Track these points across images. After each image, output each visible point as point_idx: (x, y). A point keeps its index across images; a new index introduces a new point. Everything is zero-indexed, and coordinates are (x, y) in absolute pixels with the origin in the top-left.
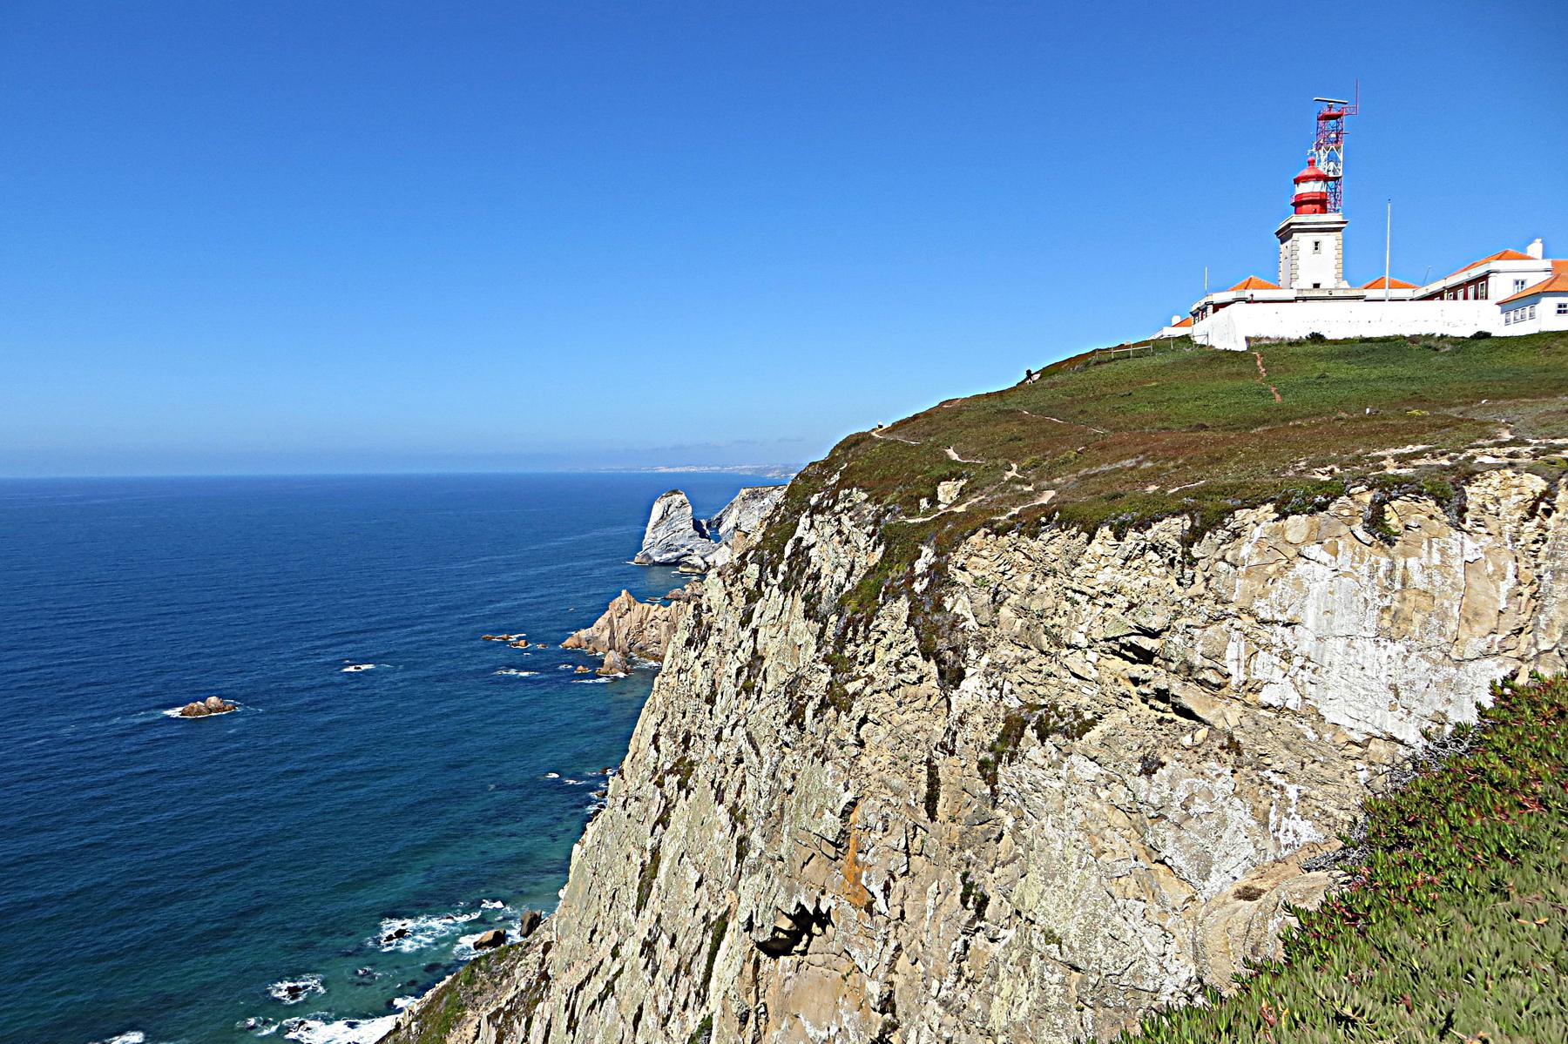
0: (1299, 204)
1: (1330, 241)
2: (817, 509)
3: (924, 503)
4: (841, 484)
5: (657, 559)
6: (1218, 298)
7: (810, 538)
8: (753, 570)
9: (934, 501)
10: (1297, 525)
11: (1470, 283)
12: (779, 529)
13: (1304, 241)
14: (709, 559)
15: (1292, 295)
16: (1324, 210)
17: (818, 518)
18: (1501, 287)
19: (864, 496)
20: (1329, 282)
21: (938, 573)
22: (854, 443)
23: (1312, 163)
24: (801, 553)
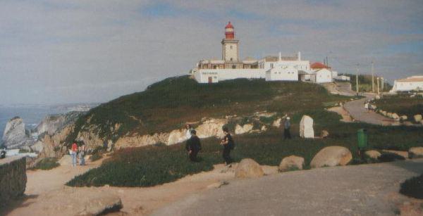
0: (227, 34)
1: (234, 46)
2: (84, 130)
4: (92, 122)
9: (114, 128)
14: (33, 147)
15: (222, 62)
20: (235, 59)
21: (113, 146)
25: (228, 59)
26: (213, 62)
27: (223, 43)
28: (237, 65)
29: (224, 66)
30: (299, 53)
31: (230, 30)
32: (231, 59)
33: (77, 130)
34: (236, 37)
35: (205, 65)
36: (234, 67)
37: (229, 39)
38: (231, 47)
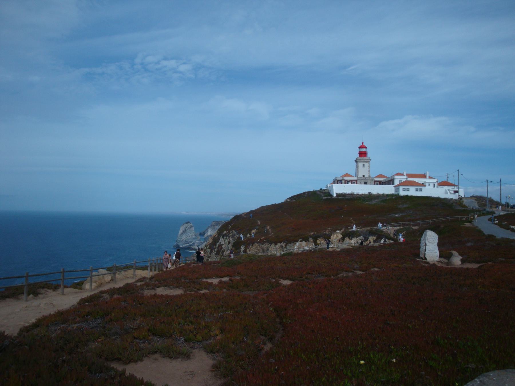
1: (366, 164)
2: (225, 235)
3: (249, 235)
5: (181, 246)
6: (338, 179)
7: (223, 242)
8: (209, 250)
9: (250, 234)
10: (304, 243)
11: (391, 180)
12: (216, 240)
13: (361, 164)
15: (355, 179)
16: (366, 156)
17: (225, 237)
18: (397, 182)
19: (235, 233)
21: (245, 251)
22: (237, 218)
23: (363, 143)
24: (221, 245)
25: (360, 175)
26: (346, 178)
27: (356, 161)
28: (369, 182)
29: (356, 182)
30: (428, 172)
31: (363, 150)
32: (364, 176)
33: (220, 233)
34: (368, 155)
35: (338, 181)
36: (366, 183)
37: (362, 158)
38: (364, 165)
